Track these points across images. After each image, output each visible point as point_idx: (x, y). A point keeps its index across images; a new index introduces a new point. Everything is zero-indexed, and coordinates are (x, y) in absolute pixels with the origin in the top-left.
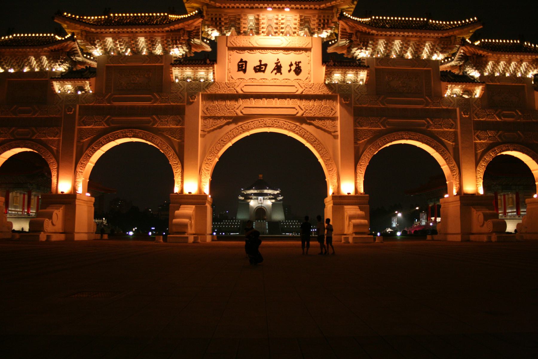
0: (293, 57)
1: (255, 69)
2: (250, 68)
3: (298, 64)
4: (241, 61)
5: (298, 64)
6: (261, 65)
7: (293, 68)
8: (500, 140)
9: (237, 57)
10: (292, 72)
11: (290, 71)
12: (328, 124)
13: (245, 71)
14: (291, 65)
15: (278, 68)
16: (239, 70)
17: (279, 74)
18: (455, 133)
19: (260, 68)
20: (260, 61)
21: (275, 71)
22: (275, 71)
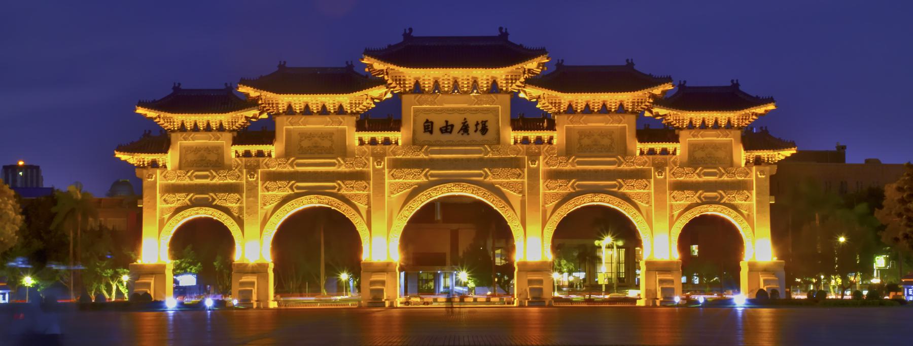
1: (441, 129)
3: (484, 123)
4: (427, 121)
5: (484, 123)
7: (480, 127)
8: (699, 201)
10: (479, 133)
11: (476, 131)
13: (431, 132)
14: (477, 124)
15: (465, 129)
16: (425, 132)
17: (465, 135)
18: (649, 194)
19: (447, 129)
20: (447, 122)
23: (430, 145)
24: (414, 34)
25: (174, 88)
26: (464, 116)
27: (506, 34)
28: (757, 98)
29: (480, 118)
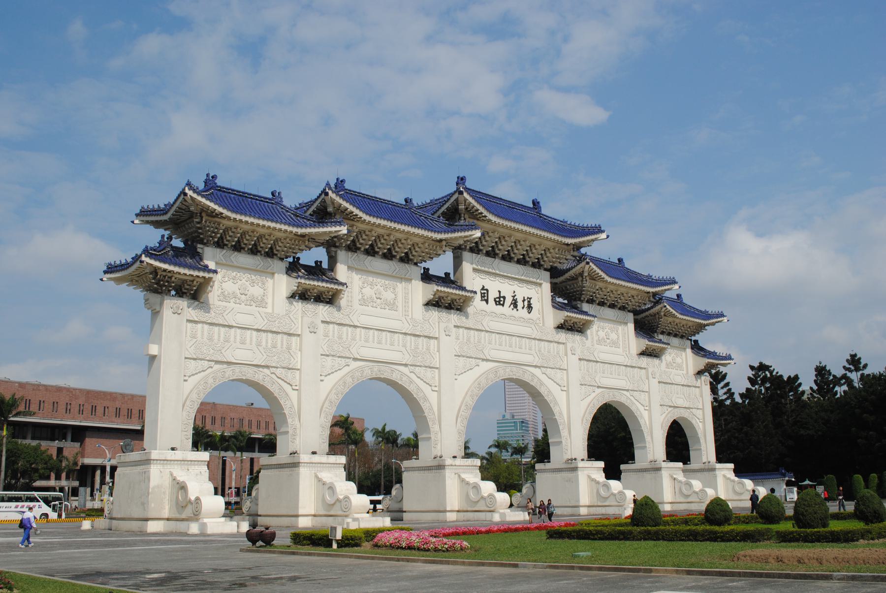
2: (491, 300)
4: (483, 289)
6: (499, 297)
7: (526, 303)
10: (525, 310)
13: (487, 301)
14: (524, 301)
15: (515, 304)
19: (500, 301)
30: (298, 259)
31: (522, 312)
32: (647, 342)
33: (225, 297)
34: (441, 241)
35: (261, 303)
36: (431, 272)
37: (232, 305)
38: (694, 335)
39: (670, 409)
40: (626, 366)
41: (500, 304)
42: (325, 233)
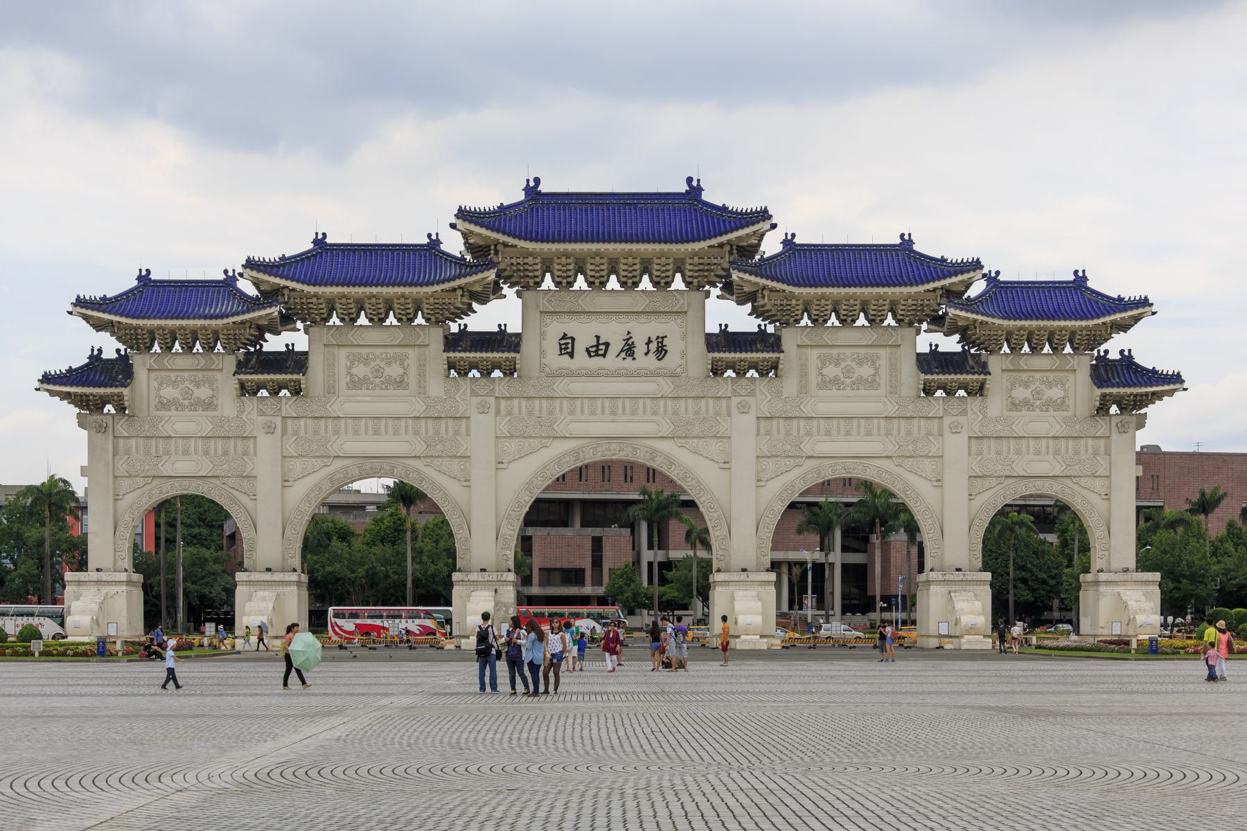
0: (654, 328)
3: (661, 340)
4: (565, 337)
5: (661, 340)
6: (598, 344)
7: (653, 347)
9: (555, 328)
10: (652, 356)
12: (714, 447)
13: (571, 355)
14: (649, 342)
15: (629, 350)
17: (630, 359)
19: (599, 349)
20: (598, 337)
21: (623, 355)
22: (623, 355)
23: (572, 374)
24: (543, 188)
25: (140, 278)
26: (628, 327)
27: (699, 190)
28: (1120, 299)
29: (654, 328)
30: (261, 346)
31: (645, 361)
32: (923, 376)
33: (164, 405)
34: (454, 290)
35: (209, 405)
36: (469, 329)
37: (173, 412)
38: (1100, 344)
39: (1009, 481)
40: (887, 418)
41: (598, 355)
42: (260, 317)
